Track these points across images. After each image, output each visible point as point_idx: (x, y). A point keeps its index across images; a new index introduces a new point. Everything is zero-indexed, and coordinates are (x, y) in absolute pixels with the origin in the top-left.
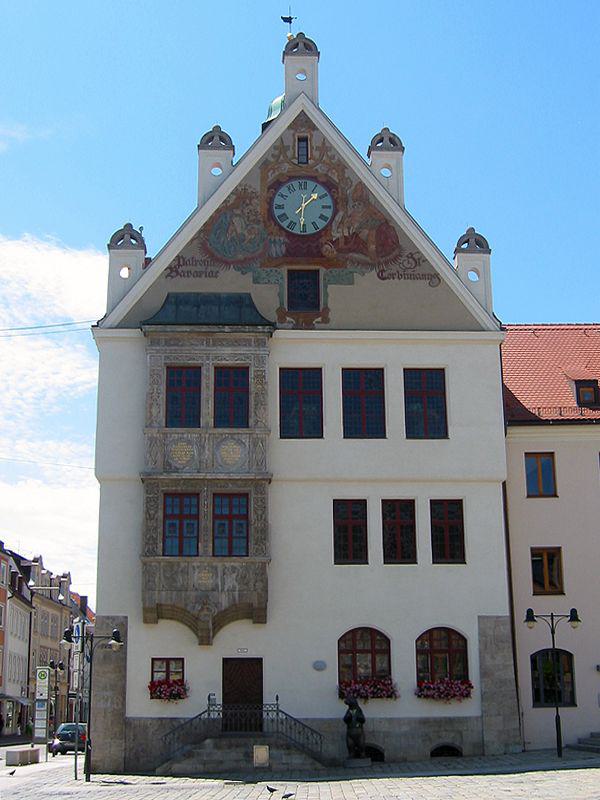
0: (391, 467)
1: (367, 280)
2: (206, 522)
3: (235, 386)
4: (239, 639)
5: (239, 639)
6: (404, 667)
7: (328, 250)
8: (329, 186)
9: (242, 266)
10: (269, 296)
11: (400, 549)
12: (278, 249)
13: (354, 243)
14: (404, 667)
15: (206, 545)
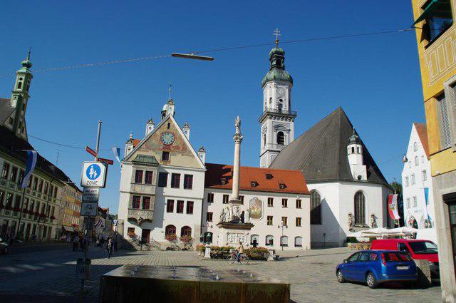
0: (180, 193)
1: (179, 156)
2: (141, 202)
3: (149, 174)
4: (147, 226)
5: (147, 226)
6: (178, 233)
7: (172, 149)
8: (173, 134)
9: (153, 150)
10: (159, 157)
11: (180, 210)
12: (161, 147)
13: (178, 147)
14: (178, 233)
15: (141, 207)
